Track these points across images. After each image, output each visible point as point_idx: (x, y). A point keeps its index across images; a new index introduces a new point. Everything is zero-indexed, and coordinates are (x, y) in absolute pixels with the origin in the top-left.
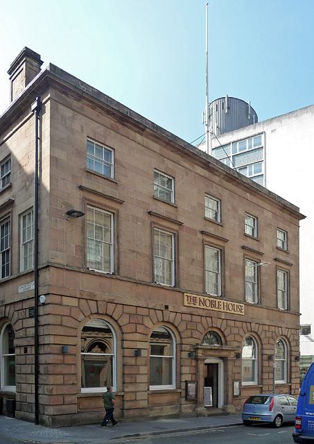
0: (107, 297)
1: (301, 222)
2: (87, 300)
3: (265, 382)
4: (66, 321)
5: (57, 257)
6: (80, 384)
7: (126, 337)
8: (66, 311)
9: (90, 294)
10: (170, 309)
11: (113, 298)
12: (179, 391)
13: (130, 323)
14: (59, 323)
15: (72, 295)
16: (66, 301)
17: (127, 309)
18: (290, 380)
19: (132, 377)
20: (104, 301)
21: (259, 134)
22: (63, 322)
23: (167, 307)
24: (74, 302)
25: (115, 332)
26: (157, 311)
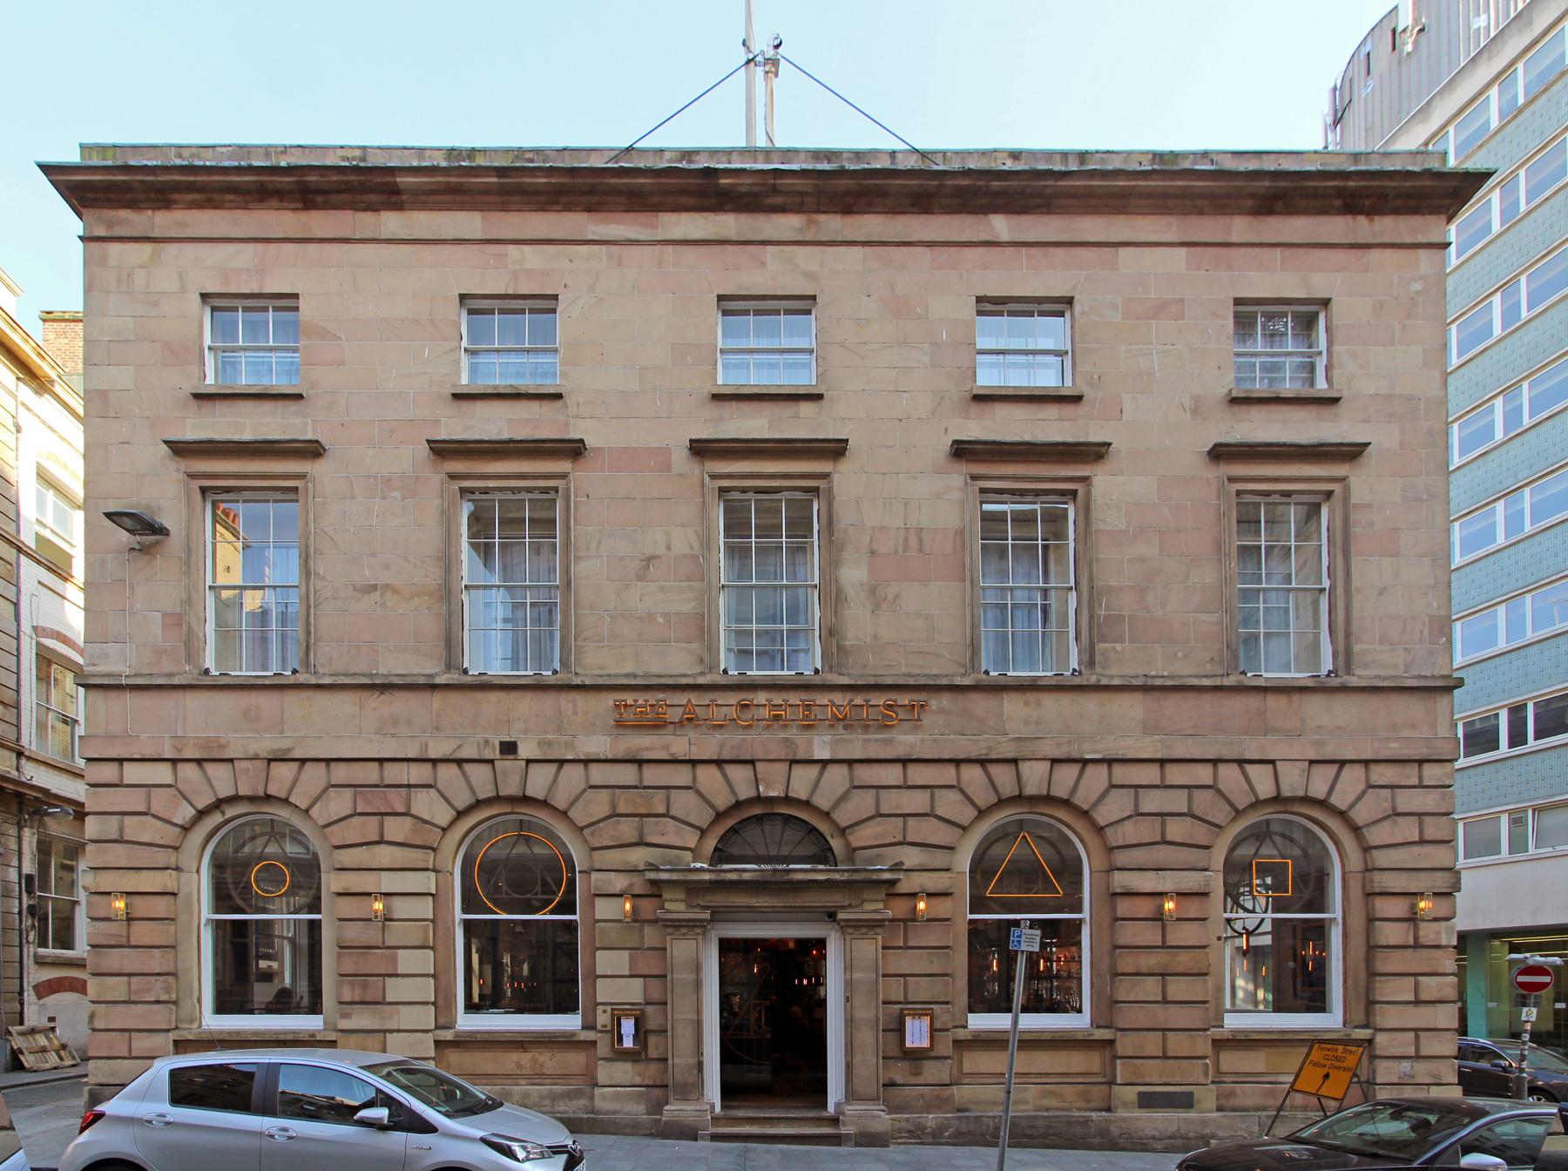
0: (267, 744)
1: (81, 234)
2: (199, 761)
3: (1388, 1017)
4: (1176, 830)
5: (107, 656)
6: (963, 999)
7: (1381, 858)
8: (134, 801)
9: (208, 743)
10: (525, 751)
11: (283, 744)
12: (589, 1035)
13: (614, 815)
14: (115, 836)
15: (148, 753)
16: (133, 773)
17: (1122, 774)
18: (1369, 1012)
19: (364, 986)
20: (256, 758)
21: (1533, 101)
22: (127, 830)
23: (509, 748)
24: (162, 773)
25: (1082, 842)
26: (1250, 768)
